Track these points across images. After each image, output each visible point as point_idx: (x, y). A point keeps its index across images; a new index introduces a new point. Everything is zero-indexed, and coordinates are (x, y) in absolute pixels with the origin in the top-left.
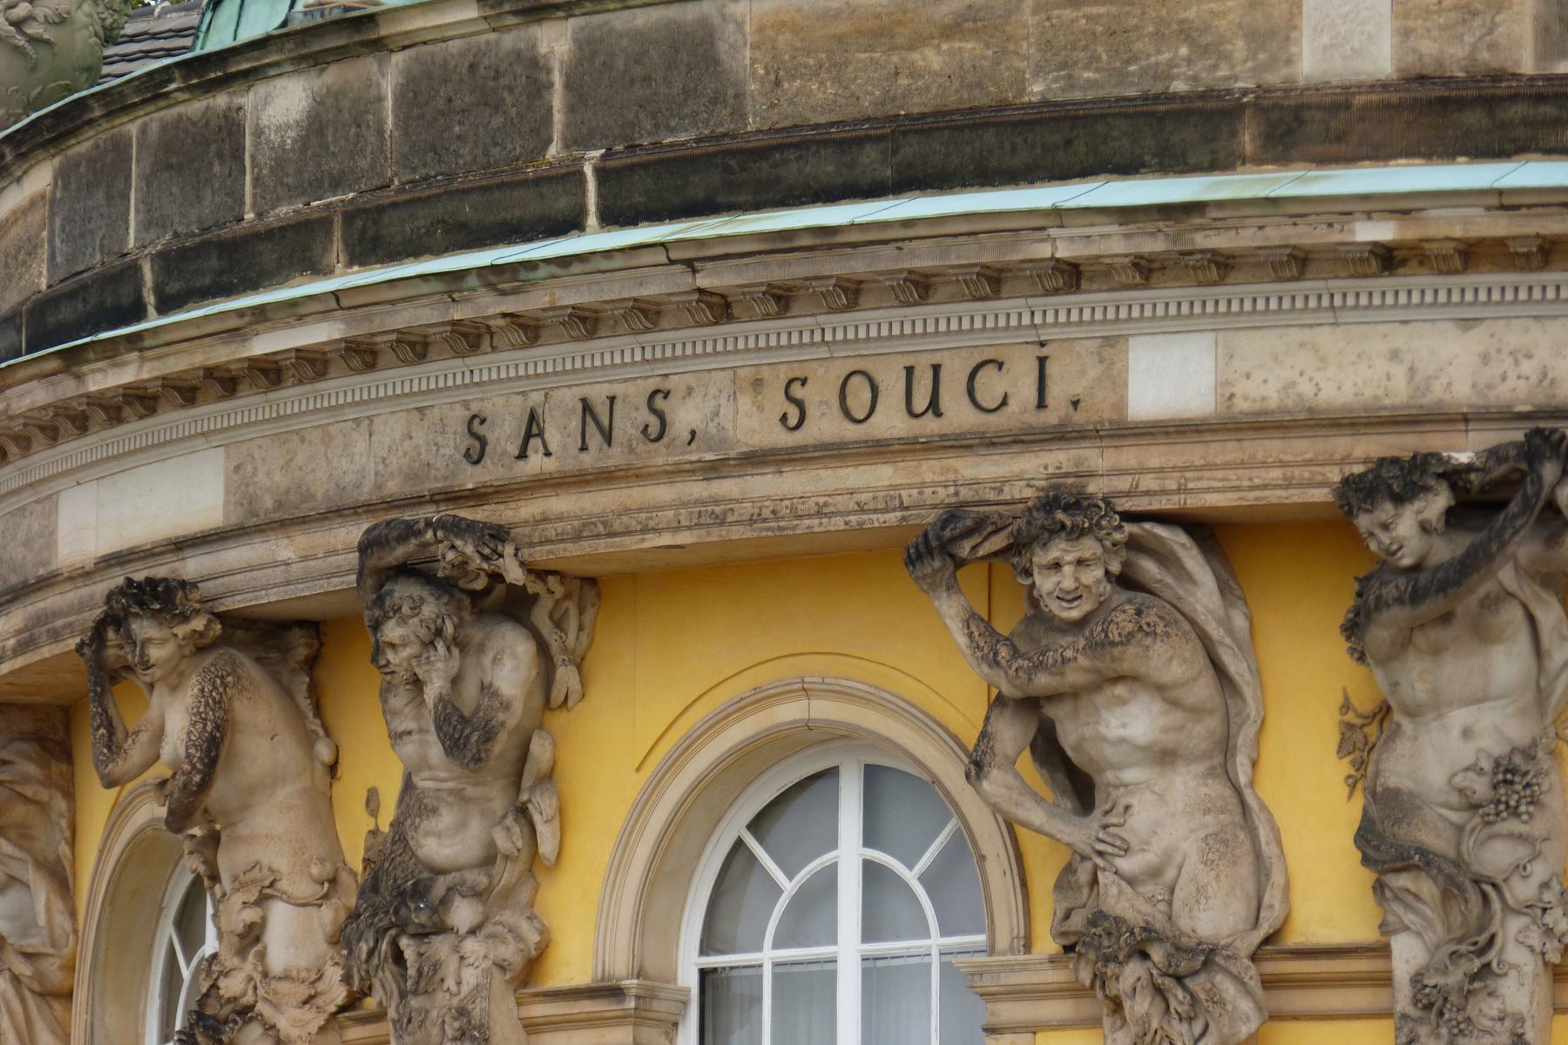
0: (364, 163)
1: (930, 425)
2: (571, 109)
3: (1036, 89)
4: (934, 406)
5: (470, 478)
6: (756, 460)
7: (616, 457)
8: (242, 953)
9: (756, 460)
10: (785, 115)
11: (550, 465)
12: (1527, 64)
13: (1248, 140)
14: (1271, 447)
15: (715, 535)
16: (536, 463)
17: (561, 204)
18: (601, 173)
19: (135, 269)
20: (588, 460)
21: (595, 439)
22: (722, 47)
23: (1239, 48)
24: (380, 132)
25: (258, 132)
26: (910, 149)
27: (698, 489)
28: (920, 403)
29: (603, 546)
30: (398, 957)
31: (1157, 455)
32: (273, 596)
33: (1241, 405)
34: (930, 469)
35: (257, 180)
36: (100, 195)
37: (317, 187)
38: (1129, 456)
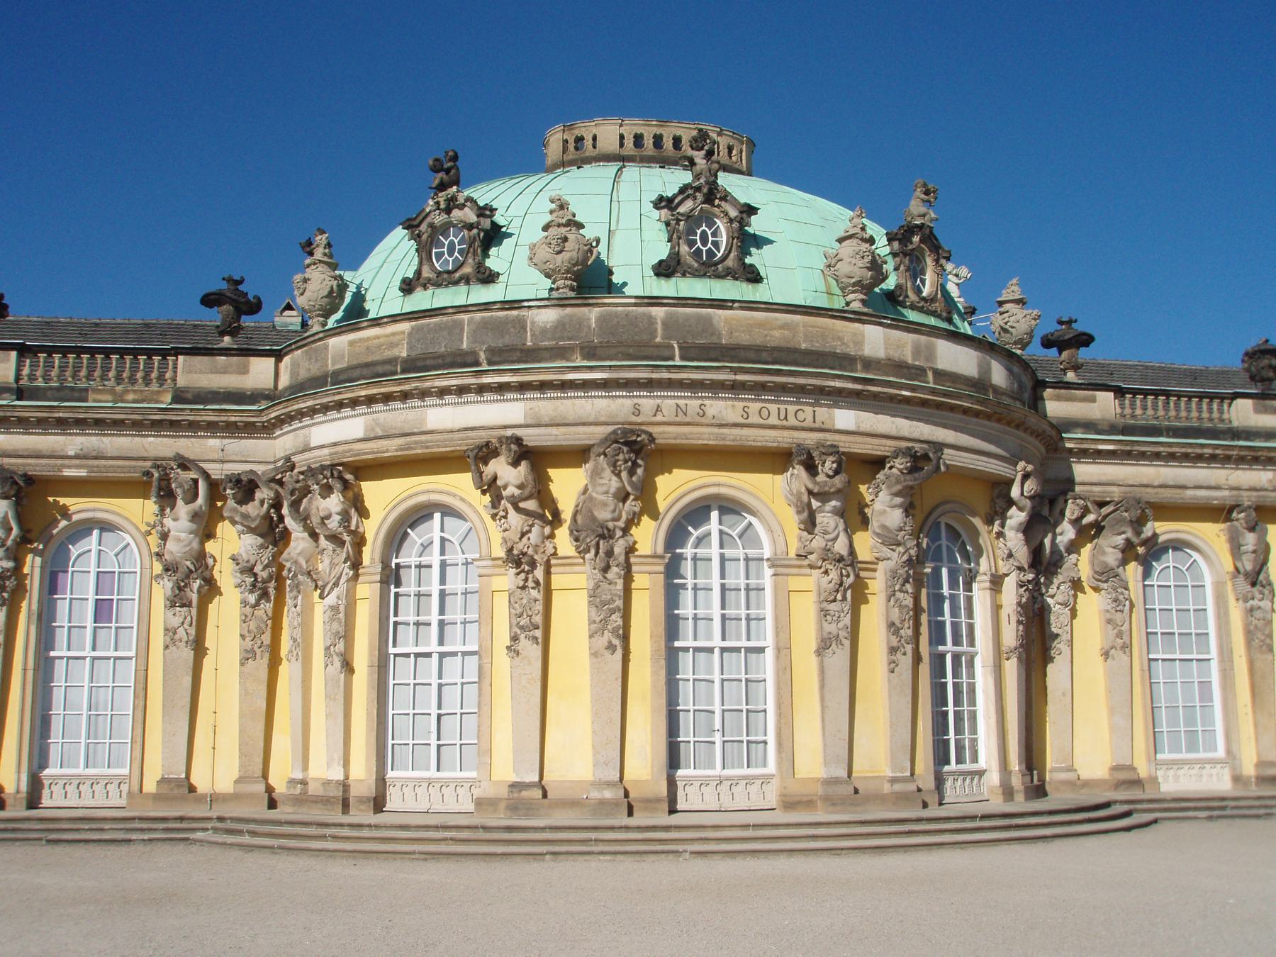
0: (583, 335)
1: (784, 423)
2: (664, 330)
3: (803, 346)
4: (786, 418)
5: (639, 420)
6: (736, 425)
7: (687, 419)
8: (520, 539)
9: (736, 425)
10: (733, 341)
11: (664, 419)
12: (910, 361)
13: (859, 367)
14: (869, 440)
15: (721, 443)
16: (659, 418)
17: (666, 353)
18: (681, 348)
19: (474, 353)
20: (678, 419)
21: (680, 413)
22: (715, 322)
23: (852, 345)
24: (589, 327)
25: (533, 323)
26: (775, 355)
27: (716, 430)
28: (782, 417)
29: (684, 442)
30: (598, 544)
31: (843, 438)
32: (550, 444)
33: (862, 429)
34: (786, 433)
35: (532, 335)
36: (445, 333)
37: (562, 339)
38: (837, 437)
